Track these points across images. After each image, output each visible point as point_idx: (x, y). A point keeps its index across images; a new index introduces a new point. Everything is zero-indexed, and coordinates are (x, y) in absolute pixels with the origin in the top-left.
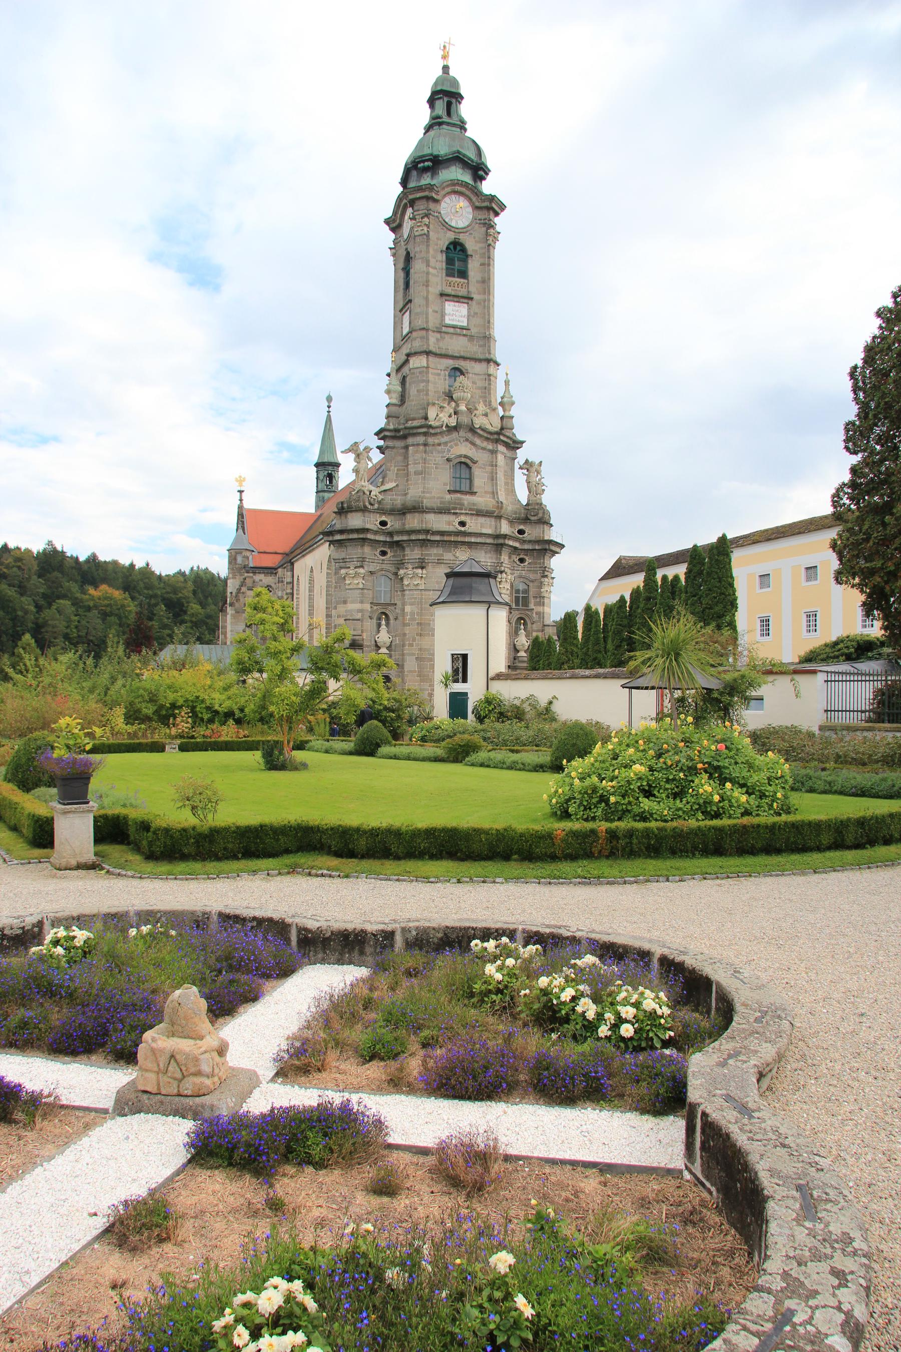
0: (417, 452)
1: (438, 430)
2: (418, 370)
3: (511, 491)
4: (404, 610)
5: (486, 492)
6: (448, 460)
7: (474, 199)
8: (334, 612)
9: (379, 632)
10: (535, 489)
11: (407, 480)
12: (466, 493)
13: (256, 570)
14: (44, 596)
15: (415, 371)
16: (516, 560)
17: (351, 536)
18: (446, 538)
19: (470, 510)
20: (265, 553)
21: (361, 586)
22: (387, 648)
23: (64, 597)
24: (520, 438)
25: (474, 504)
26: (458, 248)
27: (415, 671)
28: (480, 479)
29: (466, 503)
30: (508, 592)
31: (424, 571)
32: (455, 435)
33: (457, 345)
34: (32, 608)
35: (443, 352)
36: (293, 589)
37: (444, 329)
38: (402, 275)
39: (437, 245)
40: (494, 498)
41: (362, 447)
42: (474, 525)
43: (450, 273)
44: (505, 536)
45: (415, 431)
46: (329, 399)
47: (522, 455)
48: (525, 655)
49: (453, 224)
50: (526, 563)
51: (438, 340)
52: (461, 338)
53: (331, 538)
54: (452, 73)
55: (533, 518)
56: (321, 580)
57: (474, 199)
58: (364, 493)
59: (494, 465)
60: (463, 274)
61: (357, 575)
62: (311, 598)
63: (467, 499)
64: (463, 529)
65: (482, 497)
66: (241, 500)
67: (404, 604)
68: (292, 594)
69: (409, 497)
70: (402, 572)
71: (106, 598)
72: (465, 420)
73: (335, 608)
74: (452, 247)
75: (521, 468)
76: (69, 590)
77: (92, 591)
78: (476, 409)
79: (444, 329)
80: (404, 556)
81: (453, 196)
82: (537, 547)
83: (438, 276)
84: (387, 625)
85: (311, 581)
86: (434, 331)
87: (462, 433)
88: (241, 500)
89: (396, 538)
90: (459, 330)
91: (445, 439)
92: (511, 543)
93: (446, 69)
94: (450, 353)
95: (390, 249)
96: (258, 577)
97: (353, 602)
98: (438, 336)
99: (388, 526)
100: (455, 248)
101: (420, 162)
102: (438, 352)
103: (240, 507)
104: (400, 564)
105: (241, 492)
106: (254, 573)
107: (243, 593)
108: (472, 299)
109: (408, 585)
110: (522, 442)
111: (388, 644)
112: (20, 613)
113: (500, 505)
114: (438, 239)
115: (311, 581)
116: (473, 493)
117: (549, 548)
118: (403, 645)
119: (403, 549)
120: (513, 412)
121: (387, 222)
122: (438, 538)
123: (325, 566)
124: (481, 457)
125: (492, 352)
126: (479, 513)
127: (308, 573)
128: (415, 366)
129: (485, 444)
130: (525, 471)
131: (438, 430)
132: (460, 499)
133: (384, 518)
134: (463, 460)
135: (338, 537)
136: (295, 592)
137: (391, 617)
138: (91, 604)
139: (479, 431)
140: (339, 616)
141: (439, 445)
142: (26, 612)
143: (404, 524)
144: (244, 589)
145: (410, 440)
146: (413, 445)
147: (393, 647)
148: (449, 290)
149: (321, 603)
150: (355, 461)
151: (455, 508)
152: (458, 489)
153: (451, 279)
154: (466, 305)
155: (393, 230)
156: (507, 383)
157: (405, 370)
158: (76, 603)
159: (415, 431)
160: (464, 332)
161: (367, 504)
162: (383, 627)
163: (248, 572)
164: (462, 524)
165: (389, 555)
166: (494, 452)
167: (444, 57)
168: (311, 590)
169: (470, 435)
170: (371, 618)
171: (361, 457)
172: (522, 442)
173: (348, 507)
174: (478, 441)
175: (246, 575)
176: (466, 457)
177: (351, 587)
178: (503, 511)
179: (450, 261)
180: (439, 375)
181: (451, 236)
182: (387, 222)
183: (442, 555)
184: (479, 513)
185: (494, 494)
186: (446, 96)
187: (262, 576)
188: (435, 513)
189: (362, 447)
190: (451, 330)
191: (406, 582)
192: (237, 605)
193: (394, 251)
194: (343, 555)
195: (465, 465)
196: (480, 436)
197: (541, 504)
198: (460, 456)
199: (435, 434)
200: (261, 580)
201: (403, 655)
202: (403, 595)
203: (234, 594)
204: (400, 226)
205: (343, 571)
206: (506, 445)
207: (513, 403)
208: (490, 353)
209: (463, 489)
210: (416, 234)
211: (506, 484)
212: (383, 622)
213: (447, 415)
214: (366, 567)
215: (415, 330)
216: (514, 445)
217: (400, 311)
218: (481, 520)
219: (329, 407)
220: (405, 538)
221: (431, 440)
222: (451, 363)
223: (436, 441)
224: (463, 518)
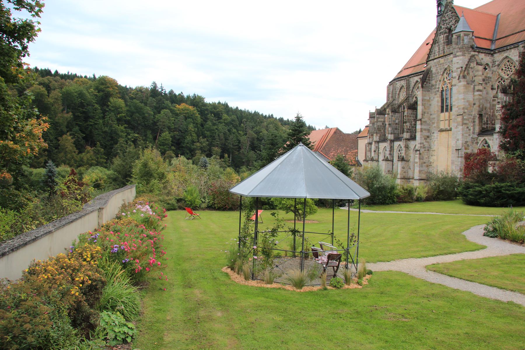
13: (480, 50)
14: (156, 108)
20: (479, 38)
23: (166, 108)
34: (152, 113)
71: (186, 109)
76: (168, 105)
77: (177, 106)
107: (472, 68)
112: (146, 115)
138: (178, 112)
142: (149, 114)
144: (472, 65)
158: (172, 111)
163: (475, 51)
175: (473, 53)
192: (468, 77)
200: (482, 59)
203: (464, 69)
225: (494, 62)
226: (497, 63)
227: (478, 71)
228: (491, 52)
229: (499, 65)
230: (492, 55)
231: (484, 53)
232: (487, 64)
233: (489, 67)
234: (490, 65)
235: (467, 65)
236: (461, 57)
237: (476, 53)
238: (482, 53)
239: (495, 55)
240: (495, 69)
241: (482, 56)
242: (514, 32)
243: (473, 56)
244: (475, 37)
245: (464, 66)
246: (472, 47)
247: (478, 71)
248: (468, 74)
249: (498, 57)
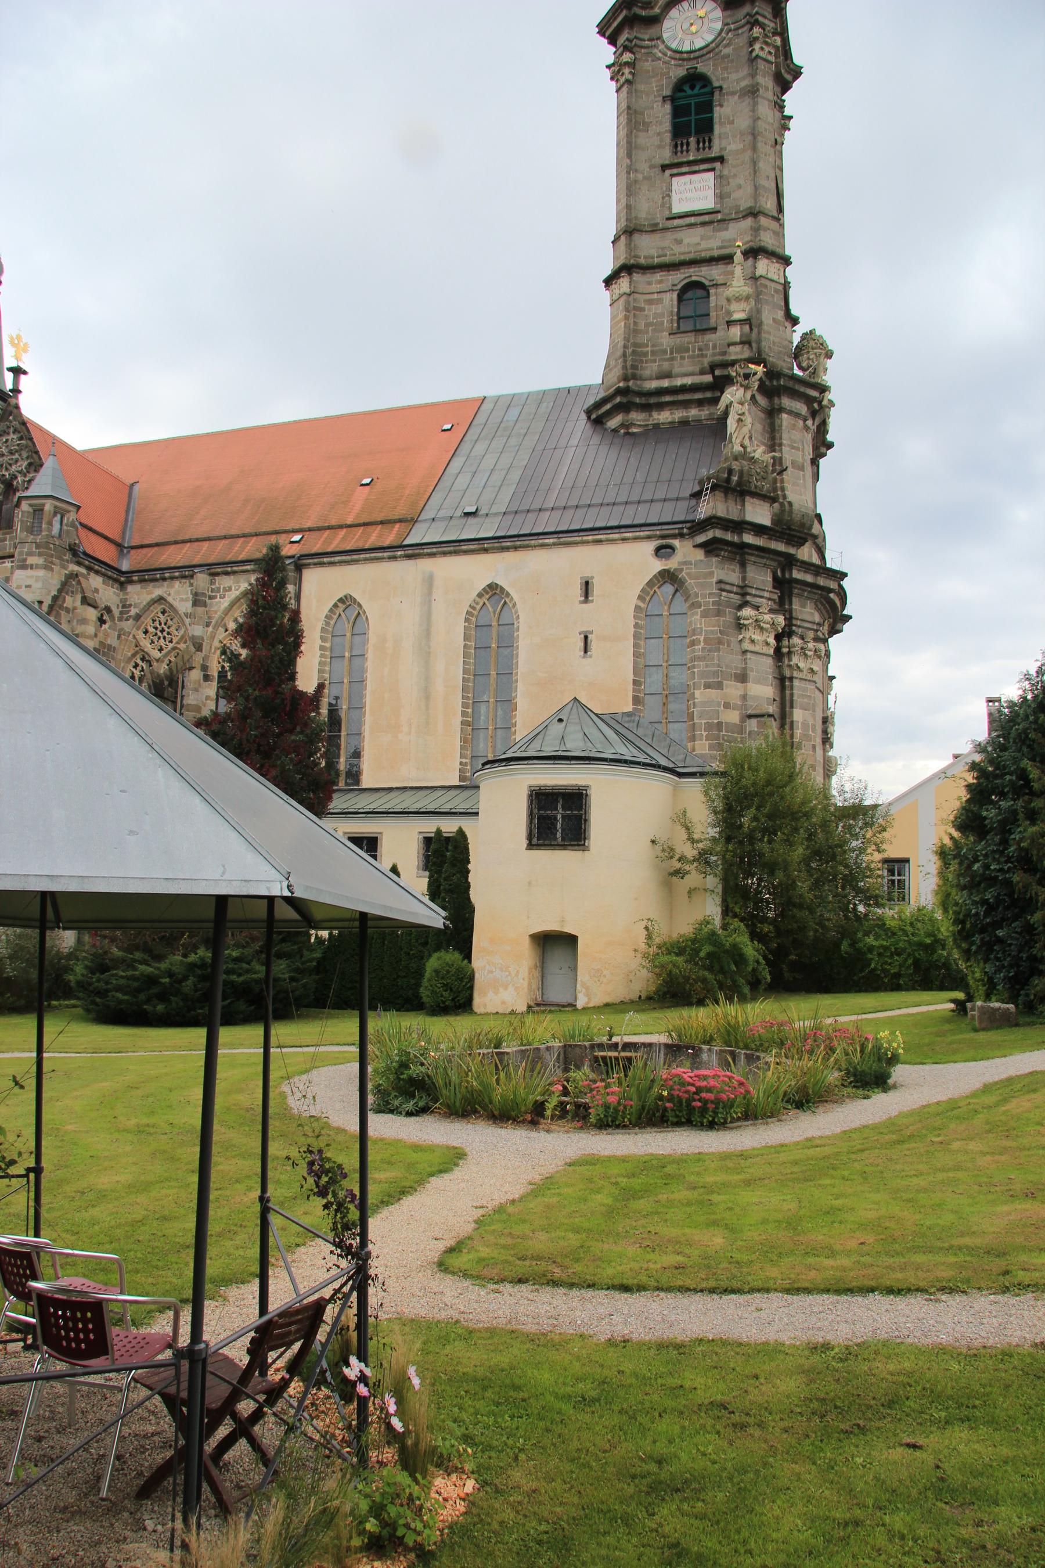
0: (794, 427)
2: (773, 285)
15: (768, 283)
20: (90, 529)
45: (802, 389)
97: (758, 681)
107: (68, 610)
140: (727, 706)
144: (69, 601)
159: (802, 389)
163: (79, 564)
173: (739, 483)
175: (75, 568)
177: (757, 648)
200: (97, 591)
220: (809, 578)
225: (125, 606)
226: (133, 611)
227: (84, 621)
228: (121, 579)
229: (138, 617)
230: (122, 585)
231: (104, 575)
232: (108, 609)
234: (116, 612)
235: (55, 599)
236: (41, 573)
237: (84, 571)
238: (97, 572)
239: (130, 588)
240: (128, 625)
241: (95, 581)
242: (180, 538)
243: (74, 576)
244: (81, 524)
245: (48, 602)
246: (73, 550)
247: (84, 621)
249: (139, 595)
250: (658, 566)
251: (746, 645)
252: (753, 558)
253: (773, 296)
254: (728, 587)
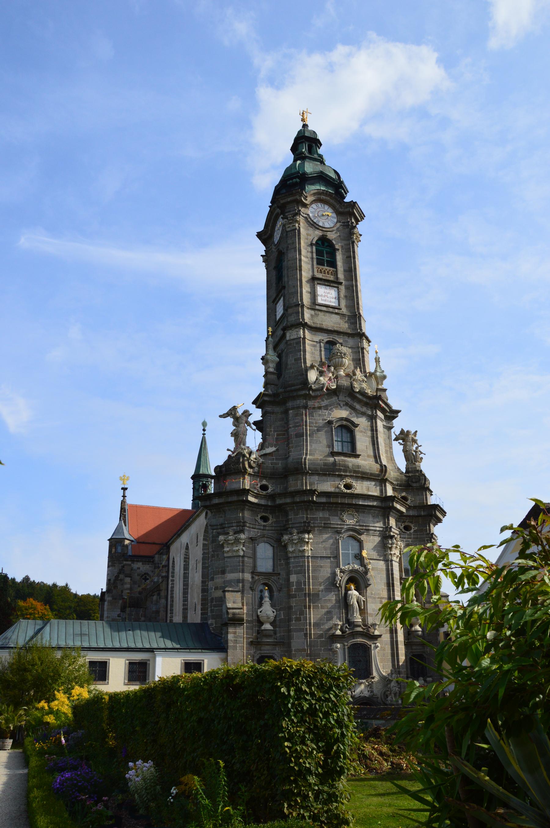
1: (318, 393)
3: (392, 459)
4: (288, 579)
5: (369, 456)
6: (330, 423)
7: (338, 206)
8: (211, 584)
9: (260, 605)
10: (412, 458)
11: (288, 444)
12: (350, 456)
16: (402, 527)
17: (230, 499)
18: (332, 500)
19: (355, 472)
21: (241, 553)
22: (271, 624)
24: (395, 408)
25: (359, 466)
26: (326, 244)
27: (304, 650)
28: (363, 442)
29: (350, 465)
30: (398, 560)
31: (311, 536)
32: (334, 399)
33: (331, 322)
35: (318, 326)
36: (168, 572)
37: (317, 307)
38: (274, 273)
39: (307, 239)
40: (376, 462)
41: (240, 412)
42: (361, 487)
43: (320, 262)
44: (392, 499)
46: (204, 424)
47: (398, 425)
48: (420, 629)
49: (321, 224)
50: (412, 531)
51: (312, 315)
52: (334, 316)
53: (208, 503)
54: (310, 128)
55: (414, 485)
56: (197, 553)
57: (338, 206)
58: (244, 456)
59: (374, 430)
60: (333, 264)
61: (237, 541)
62: (186, 576)
63: (351, 461)
64: (348, 491)
65: (365, 460)
66: (124, 496)
67: (288, 574)
68: (167, 577)
69: (290, 459)
70: (286, 537)
72: (345, 383)
73: (212, 579)
74: (320, 242)
75: (396, 439)
78: (354, 374)
79: (317, 307)
80: (287, 521)
81: (319, 204)
82: (422, 513)
83: (308, 264)
84: (271, 598)
85: (187, 559)
86: (308, 308)
87: (341, 397)
88: (124, 496)
89: (279, 501)
90: (331, 310)
91: (325, 403)
92: (398, 507)
93: (305, 126)
94: (325, 327)
95: (261, 256)
96: (136, 566)
97: (232, 572)
98: (313, 312)
99: (269, 490)
100: (323, 244)
101: (289, 180)
102: (313, 325)
103: (123, 502)
104: (284, 529)
105: (124, 489)
106: (133, 561)
108: (341, 283)
109: (293, 552)
110: (398, 412)
111: (272, 619)
113: (383, 469)
114: (308, 234)
115: (187, 559)
116: (358, 456)
117: (434, 514)
118: (290, 620)
119: (287, 514)
120: (385, 384)
121: (260, 235)
122: (323, 500)
123: (201, 538)
124: (362, 422)
125: (363, 328)
126: (364, 476)
127: (183, 551)
128: (292, 338)
129: (364, 409)
130: (401, 441)
131: (318, 393)
132: (345, 461)
133: (264, 482)
134: (345, 423)
135: (216, 501)
136: (170, 575)
137: (275, 589)
139: (358, 395)
140: (216, 588)
141: (320, 408)
143: (286, 488)
144: (121, 576)
145: (290, 404)
146: (293, 408)
147: (278, 623)
148: (320, 276)
149: (196, 577)
150: (234, 425)
151: (340, 470)
152: (340, 451)
153: (321, 267)
154: (336, 289)
155: (264, 242)
156: (377, 360)
157: (282, 346)
160: (336, 311)
161: (247, 466)
162: (267, 600)
163: (127, 561)
164: (348, 486)
165: (270, 522)
166: (373, 418)
167: (303, 120)
168: (186, 568)
169: (349, 400)
170: (252, 589)
171: (240, 420)
172: (398, 412)
174: (358, 406)
175: (125, 562)
176: (347, 420)
177: (230, 554)
178: (387, 474)
179: (319, 253)
180: (314, 346)
181: (319, 233)
182: (260, 235)
183: (329, 519)
184: (364, 476)
185: (377, 458)
186: (307, 141)
187: (140, 565)
188: (319, 474)
189: (240, 412)
190: (324, 309)
191: (290, 549)
193: (266, 258)
194: (221, 520)
195: (348, 428)
196: (359, 401)
197: (421, 471)
198: (342, 419)
199: (315, 397)
200: (139, 568)
201: (289, 631)
202: (288, 564)
204: (271, 236)
205: (221, 538)
206: (383, 411)
207: (384, 377)
208: (361, 330)
209: (345, 451)
210: (288, 229)
211: (386, 452)
212: (266, 594)
213: (327, 379)
214: (246, 533)
215: (291, 307)
216: (392, 415)
217: (273, 302)
218: (366, 484)
219: (204, 430)
220: (288, 500)
221: (310, 403)
222: (325, 338)
223: (317, 405)
224: (349, 480)
231: (142, 561)
233: (150, 577)
237: (130, 563)
238: (138, 561)
248: (115, 587)
250: (205, 523)
251: (226, 555)
252: (227, 508)
253: (295, 347)
254: (215, 527)
